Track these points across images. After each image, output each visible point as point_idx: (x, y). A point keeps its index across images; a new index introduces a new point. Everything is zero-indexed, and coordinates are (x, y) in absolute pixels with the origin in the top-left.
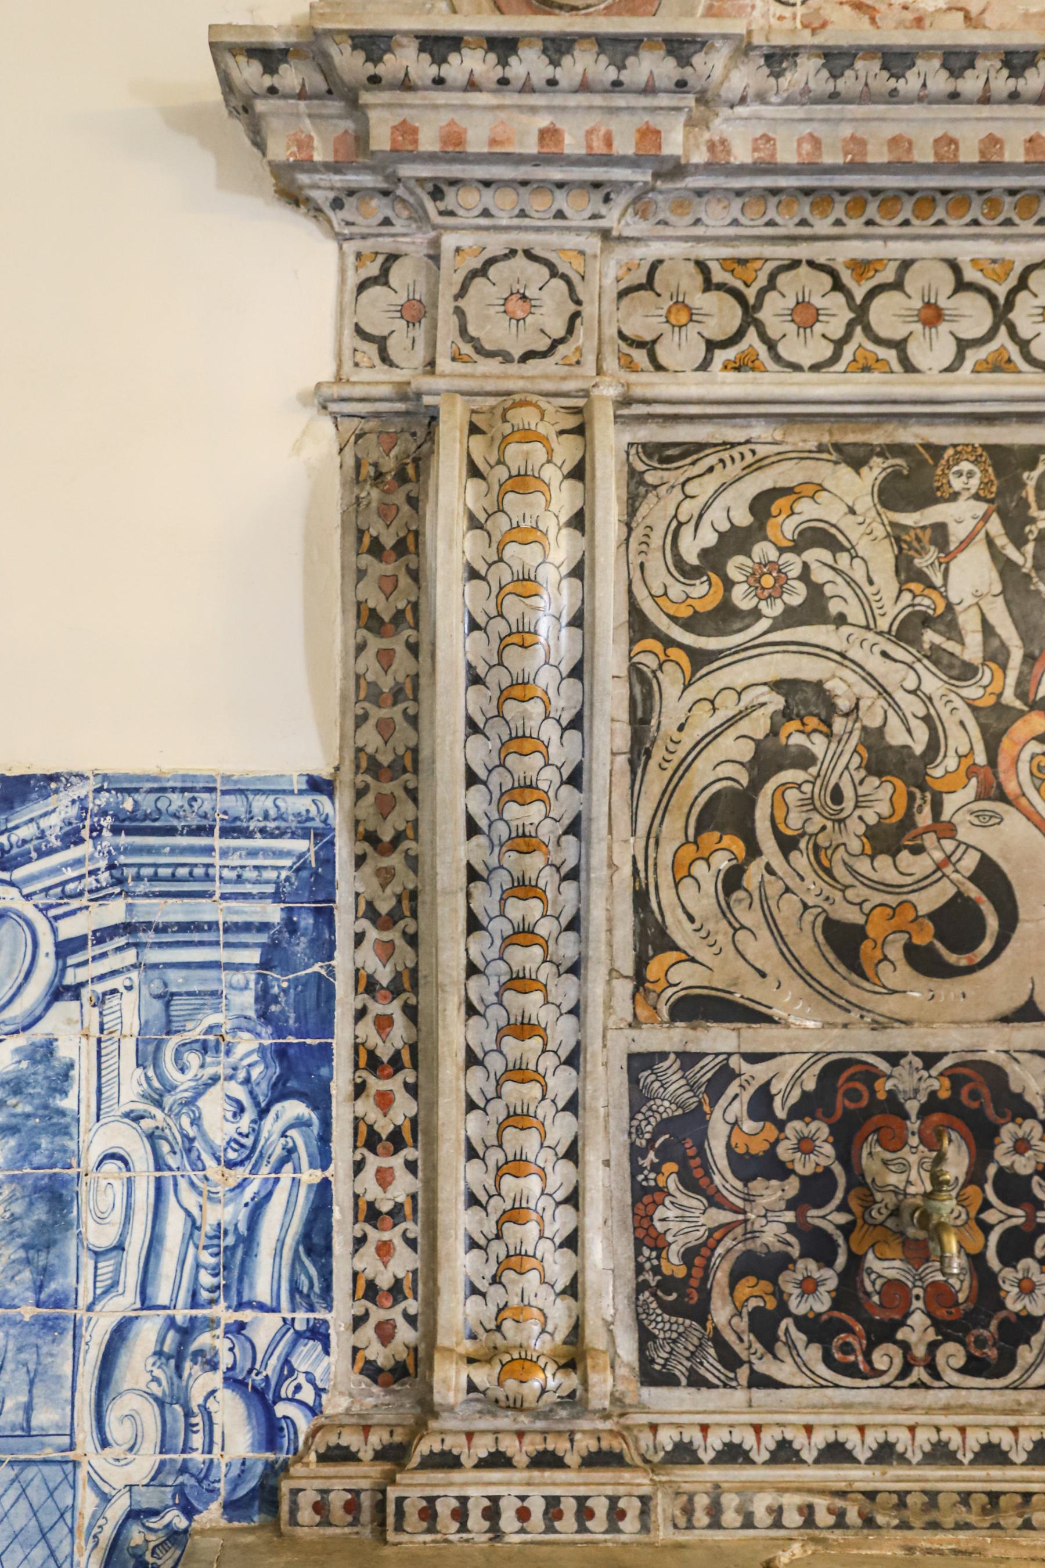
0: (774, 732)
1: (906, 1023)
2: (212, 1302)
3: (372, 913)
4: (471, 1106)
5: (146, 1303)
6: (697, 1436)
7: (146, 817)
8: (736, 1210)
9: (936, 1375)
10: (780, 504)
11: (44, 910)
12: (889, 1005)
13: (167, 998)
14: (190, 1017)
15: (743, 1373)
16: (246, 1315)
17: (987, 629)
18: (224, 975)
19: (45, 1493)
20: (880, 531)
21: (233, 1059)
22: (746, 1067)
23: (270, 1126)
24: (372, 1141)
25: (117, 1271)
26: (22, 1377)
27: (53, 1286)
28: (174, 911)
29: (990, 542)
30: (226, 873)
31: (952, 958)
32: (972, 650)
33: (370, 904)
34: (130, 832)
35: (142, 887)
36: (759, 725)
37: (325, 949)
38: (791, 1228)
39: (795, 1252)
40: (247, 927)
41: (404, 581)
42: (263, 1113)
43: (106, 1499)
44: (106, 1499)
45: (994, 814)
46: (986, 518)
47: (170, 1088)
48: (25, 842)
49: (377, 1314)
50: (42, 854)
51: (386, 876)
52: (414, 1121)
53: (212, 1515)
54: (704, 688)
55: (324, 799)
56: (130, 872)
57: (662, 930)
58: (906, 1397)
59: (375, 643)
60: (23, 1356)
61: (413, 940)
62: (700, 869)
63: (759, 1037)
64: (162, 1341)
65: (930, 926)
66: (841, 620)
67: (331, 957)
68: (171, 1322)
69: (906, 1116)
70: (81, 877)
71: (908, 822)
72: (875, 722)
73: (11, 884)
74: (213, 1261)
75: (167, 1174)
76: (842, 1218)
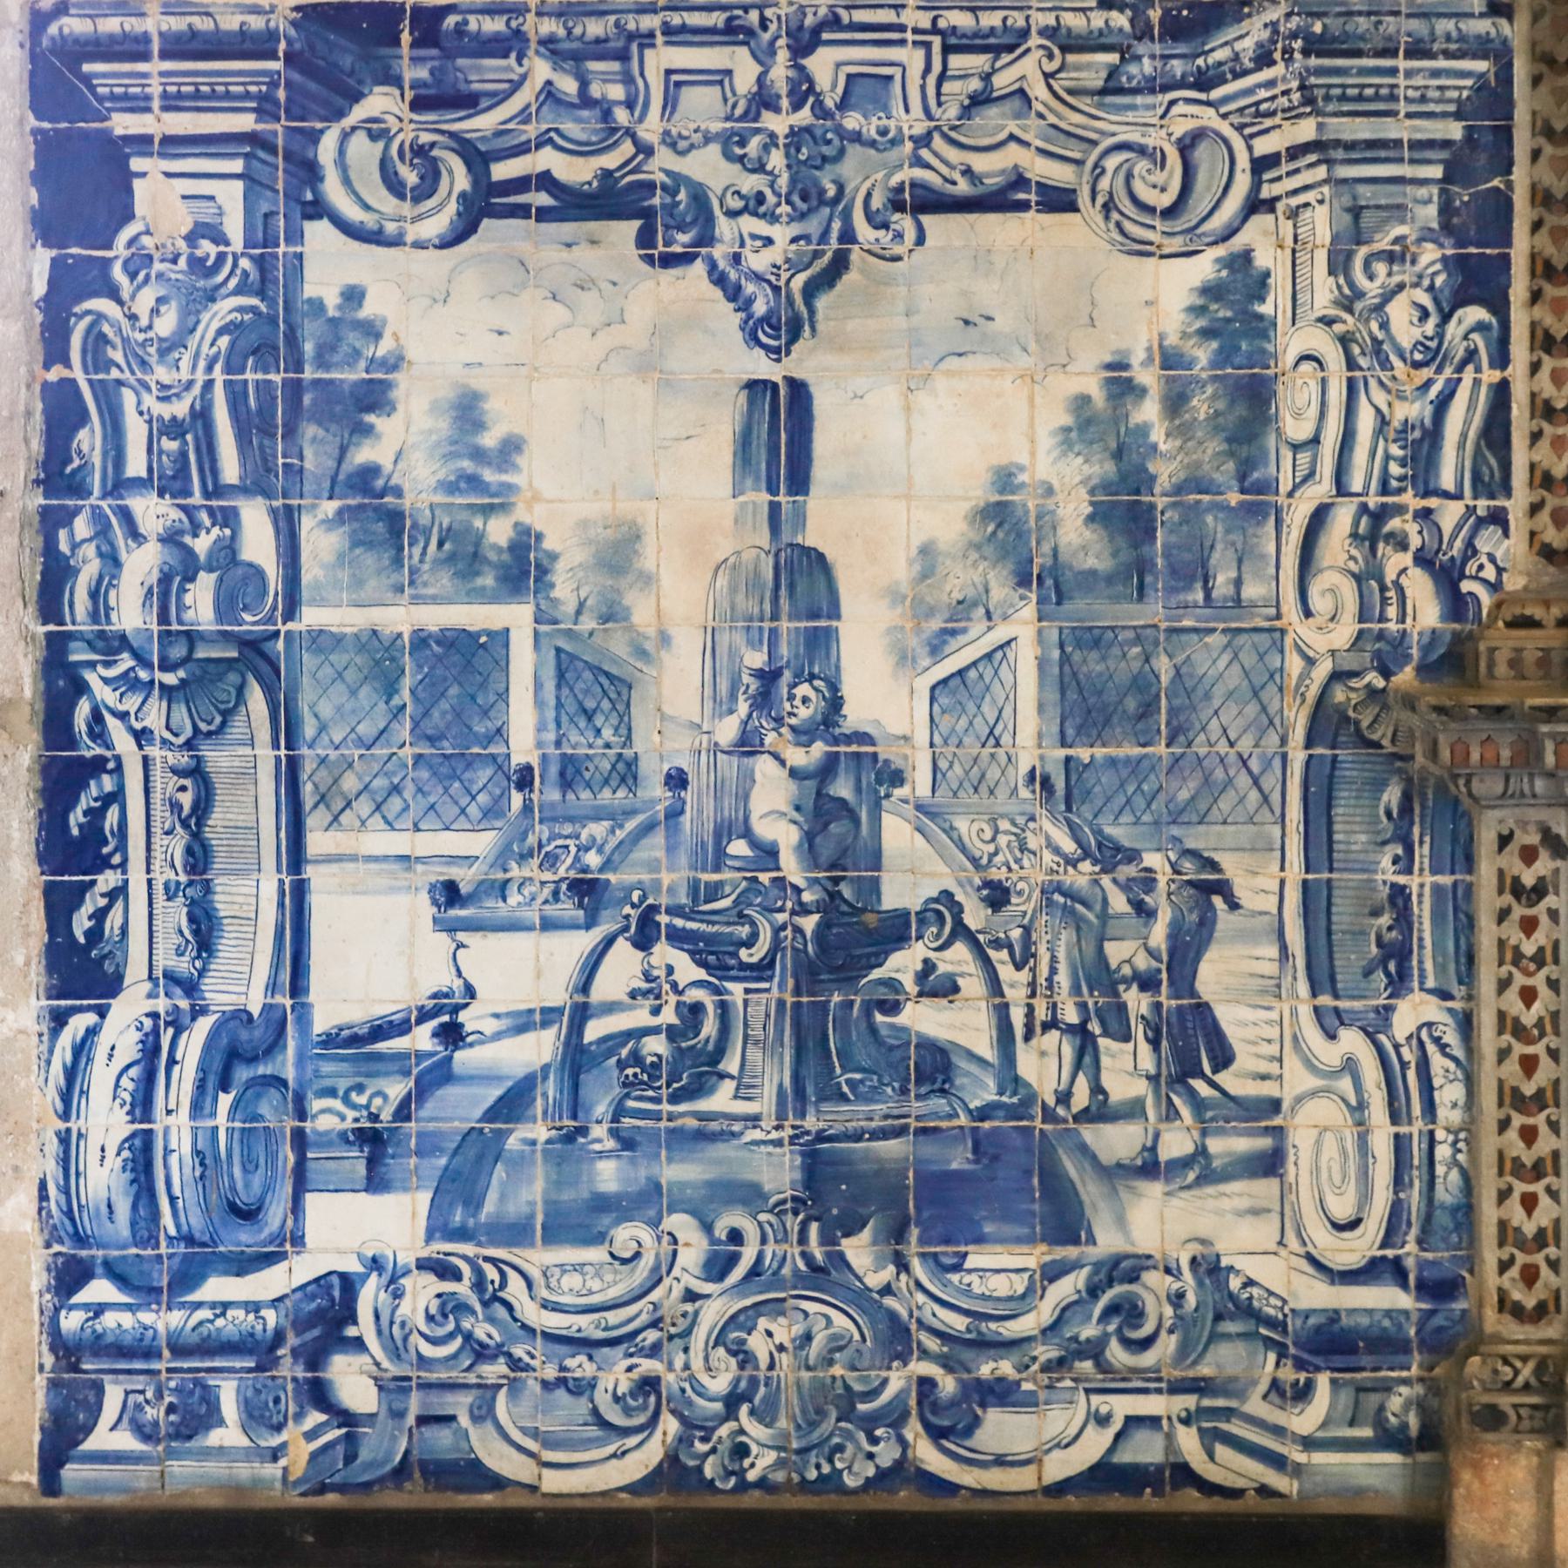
2: (1400, 491)
3: (1548, 132)
5: (1341, 489)
7: (1334, 39)
11: (1240, 128)
13: (1356, 212)
16: (1433, 502)
18: (1409, 189)
19: (1255, 658)
21: (1417, 268)
23: (1453, 330)
26: (1231, 554)
27: (1256, 475)
28: (1362, 129)
30: (1410, 93)
34: (1319, 55)
35: (1331, 108)
40: (1430, 144)
42: (1446, 318)
43: (1310, 662)
44: (1310, 662)
47: (1359, 294)
48: (1220, 64)
50: (1237, 75)
53: (1406, 677)
55: (1503, 22)
56: (1319, 93)
60: (1232, 537)
64: (1356, 523)
67: (1509, 172)
68: (1364, 508)
70: (1273, 98)
73: (1208, 104)
74: (1400, 453)
75: (1358, 374)
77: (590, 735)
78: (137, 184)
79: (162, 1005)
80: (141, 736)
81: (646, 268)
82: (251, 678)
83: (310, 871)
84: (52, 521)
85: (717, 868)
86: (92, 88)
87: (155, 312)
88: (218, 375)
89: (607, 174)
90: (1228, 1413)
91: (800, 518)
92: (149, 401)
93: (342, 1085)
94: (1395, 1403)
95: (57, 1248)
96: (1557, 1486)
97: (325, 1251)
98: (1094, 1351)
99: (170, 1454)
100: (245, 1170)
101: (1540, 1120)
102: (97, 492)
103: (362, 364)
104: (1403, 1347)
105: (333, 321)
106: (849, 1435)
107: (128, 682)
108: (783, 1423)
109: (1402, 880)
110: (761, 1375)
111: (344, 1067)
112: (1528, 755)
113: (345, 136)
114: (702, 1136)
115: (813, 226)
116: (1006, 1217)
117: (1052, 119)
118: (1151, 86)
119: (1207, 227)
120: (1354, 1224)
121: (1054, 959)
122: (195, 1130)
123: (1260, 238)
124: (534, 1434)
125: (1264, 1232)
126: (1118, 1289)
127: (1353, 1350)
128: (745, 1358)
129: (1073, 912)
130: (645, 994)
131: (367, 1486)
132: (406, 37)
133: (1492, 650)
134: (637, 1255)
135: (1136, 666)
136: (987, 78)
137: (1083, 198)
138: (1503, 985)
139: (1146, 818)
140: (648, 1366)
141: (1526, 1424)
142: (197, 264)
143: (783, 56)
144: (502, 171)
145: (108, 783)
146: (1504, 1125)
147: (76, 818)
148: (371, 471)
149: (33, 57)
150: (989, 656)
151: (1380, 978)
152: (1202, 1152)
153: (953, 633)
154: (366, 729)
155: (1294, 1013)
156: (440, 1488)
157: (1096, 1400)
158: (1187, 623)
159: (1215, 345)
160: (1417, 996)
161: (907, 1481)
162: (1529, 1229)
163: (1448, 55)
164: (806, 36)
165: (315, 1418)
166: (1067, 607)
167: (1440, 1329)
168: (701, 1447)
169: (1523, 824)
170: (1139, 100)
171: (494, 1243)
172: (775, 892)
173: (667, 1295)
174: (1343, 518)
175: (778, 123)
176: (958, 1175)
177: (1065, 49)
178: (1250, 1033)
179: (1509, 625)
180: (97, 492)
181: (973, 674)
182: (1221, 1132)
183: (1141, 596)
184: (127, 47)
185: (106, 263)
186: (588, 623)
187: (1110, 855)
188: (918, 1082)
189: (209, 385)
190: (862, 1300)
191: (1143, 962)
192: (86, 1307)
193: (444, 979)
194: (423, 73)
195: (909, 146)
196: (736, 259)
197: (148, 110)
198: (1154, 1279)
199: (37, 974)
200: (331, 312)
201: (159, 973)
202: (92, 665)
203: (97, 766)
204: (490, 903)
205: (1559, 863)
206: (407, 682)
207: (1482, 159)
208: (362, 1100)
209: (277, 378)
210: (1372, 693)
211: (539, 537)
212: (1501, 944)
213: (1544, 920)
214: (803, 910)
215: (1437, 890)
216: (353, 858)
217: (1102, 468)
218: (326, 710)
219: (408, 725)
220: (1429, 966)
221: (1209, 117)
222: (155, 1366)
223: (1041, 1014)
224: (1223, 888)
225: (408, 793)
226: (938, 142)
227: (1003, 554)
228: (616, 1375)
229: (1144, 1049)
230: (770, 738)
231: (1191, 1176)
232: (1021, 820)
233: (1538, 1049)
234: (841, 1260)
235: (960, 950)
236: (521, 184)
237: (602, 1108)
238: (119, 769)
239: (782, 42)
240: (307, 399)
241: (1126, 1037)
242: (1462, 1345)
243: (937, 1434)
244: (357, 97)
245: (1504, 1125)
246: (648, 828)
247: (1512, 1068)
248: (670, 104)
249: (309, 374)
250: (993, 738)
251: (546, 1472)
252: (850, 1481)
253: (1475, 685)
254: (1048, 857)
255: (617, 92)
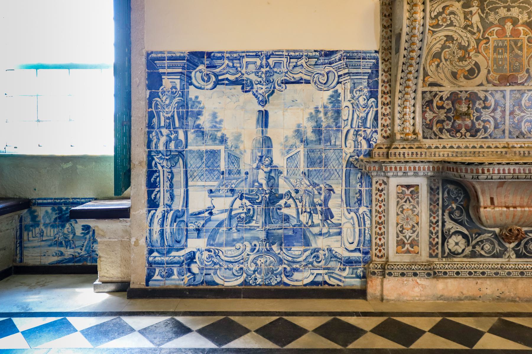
0: (445, 43)
1: (463, 86)
2: (361, 127)
3: (384, 71)
4: (399, 99)
5: (352, 127)
6: (432, 145)
8: (437, 114)
9: (466, 137)
10: (447, 8)
12: (461, 84)
13: (354, 84)
14: (358, 86)
15: (438, 137)
16: (366, 129)
17: (478, 27)
20: (462, 12)
22: (439, 93)
23: (369, 102)
24: (384, 104)
25: (347, 123)
26: (334, 138)
28: (355, 71)
29: (479, 13)
31: (470, 77)
32: (475, 30)
33: (384, 70)
35: (350, 67)
36: (442, 42)
37: (378, 76)
38: (445, 116)
39: (446, 120)
40: (366, 73)
41: (390, 20)
42: (368, 100)
43: (347, 154)
44: (347, 154)
45: (477, 55)
46: (478, 10)
47: (354, 97)
49: (385, 129)
50: (336, 62)
51: (386, 65)
52: (390, 101)
53: (361, 157)
54: (434, 37)
55: (377, 54)
56: (348, 65)
57: (427, 73)
58: (461, 140)
59: (385, 30)
61: (390, 75)
62: (433, 64)
63: (441, 89)
64: (354, 133)
65: (467, 72)
66: (455, 26)
68: (355, 130)
69: (463, 100)
71: (464, 56)
72: (460, 41)
76: (453, 115)
77: (233, 166)
78: (163, 80)
79: (165, 209)
80: (163, 167)
81: (243, 93)
82: (180, 157)
83: (189, 188)
84: (149, 133)
85: (253, 187)
86: (156, 65)
87: (166, 100)
88: (175, 110)
89: (237, 78)
90: (333, 273)
91: (267, 132)
92: (164, 114)
93: (194, 222)
94: (359, 271)
95: (149, 247)
96: (384, 284)
97: (191, 248)
98: (312, 263)
99: (166, 280)
100: (178, 235)
101: (382, 226)
102: (156, 128)
103: (198, 108)
104: (360, 262)
105: (194, 102)
106: (273, 277)
107: (161, 158)
108: (262, 275)
109: (361, 189)
110: (259, 267)
111: (194, 219)
112: (380, 169)
113: (196, 72)
114: (250, 229)
115: (269, 86)
116: (298, 242)
117: (307, 69)
118: (322, 64)
119: (330, 86)
120: (353, 243)
121: (306, 201)
122: (170, 229)
123: (339, 88)
124: (223, 276)
125: (339, 244)
126: (315, 253)
127: (352, 263)
128: (256, 264)
129: (309, 194)
130: (241, 207)
131: (197, 285)
132: (205, 57)
133: (375, 152)
134: (240, 248)
135: (319, 155)
136: (296, 63)
137: (311, 82)
138: (376, 205)
139: (321, 179)
140: (241, 266)
141: (379, 274)
142: (172, 92)
143: (264, 59)
144: (220, 78)
145: (157, 174)
146: (376, 227)
147: (152, 180)
148: (199, 125)
149: (147, 60)
150: (296, 154)
151: (357, 204)
152: (329, 232)
153: (290, 150)
154: (198, 166)
155: (344, 210)
156: (208, 285)
157: (312, 271)
158: (327, 148)
159: (332, 104)
160: (363, 207)
161: (282, 284)
162: (380, 244)
163: (368, 59)
164: (268, 56)
165: (189, 274)
166: (308, 146)
167: (366, 260)
168: (250, 279)
169: (380, 180)
170: (320, 66)
171: (217, 246)
172: (262, 191)
173: (244, 255)
174: (352, 131)
175: (263, 70)
176: (291, 236)
177: (309, 58)
178: (337, 213)
179: (378, 148)
180: (156, 128)
181: (293, 156)
182: (332, 228)
183: (320, 144)
184: (162, 59)
185: (158, 92)
186: (233, 149)
187: (315, 185)
188: (284, 221)
189: (174, 111)
190: (275, 255)
191: (320, 202)
192: (153, 257)
193: (209, 205)
194: (208, 62)
195: (284, 73)
196: (257, 91)
197: (165, 68)
198: (321, 252)
199: (146, 204)
200: (193, 100)
201: (165, 204)
202: (155, 155)
203: (156, 171)
204: (217, 193)
205: (385, 186)
206: (204, 158)
207: (374, 75)
208: (197, 224)
209: (184, 110)
210: (356, 159)
211: (225, 135)
212: (376, 198)
213: (383, 195)
214: (266, 194)
215: (366, 190)
216: (196, 186)
217: (314, 124)
218: (192, 162)
219: (205, 165)
220: (365, 202)
221: (331, 69)
222: (164, 266)
223: (304, 210)
224: (332, 190)
225: (205, 175)
226: (289, 73)
227: (298, 137)
228: (236, 267)
229: (320, 215)
230: (261, 167)
231: (327, 235)
232: (301, 179)
233: (382, 215)
234: (272, 249)
235: (291, 200)
236: (223, 80)
237: (234, 225)
238: (159, 172)
239: (264, 57)
240: (189, 114)
241: (317, 214)
242: (369, 262)
243: (287, 276)
244: (197, 66)
245: (376, 227)
246: (242, 181)
247: (378, 218)
248: (247, 67)
249: (190, 110)
250: (296, 167)
251: (225, 283)
252: (273, 284)
253: (372, 158)
254: (305, 185)
255: (238, 65)
